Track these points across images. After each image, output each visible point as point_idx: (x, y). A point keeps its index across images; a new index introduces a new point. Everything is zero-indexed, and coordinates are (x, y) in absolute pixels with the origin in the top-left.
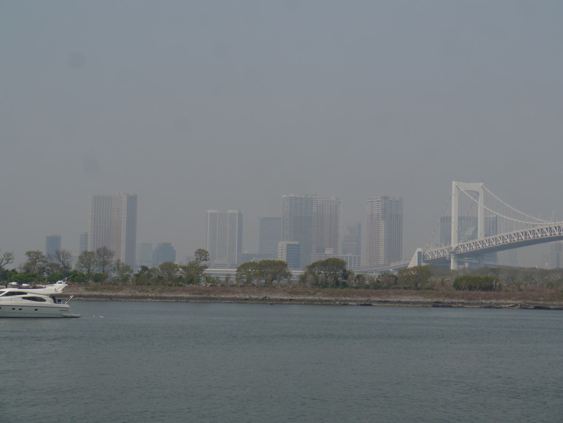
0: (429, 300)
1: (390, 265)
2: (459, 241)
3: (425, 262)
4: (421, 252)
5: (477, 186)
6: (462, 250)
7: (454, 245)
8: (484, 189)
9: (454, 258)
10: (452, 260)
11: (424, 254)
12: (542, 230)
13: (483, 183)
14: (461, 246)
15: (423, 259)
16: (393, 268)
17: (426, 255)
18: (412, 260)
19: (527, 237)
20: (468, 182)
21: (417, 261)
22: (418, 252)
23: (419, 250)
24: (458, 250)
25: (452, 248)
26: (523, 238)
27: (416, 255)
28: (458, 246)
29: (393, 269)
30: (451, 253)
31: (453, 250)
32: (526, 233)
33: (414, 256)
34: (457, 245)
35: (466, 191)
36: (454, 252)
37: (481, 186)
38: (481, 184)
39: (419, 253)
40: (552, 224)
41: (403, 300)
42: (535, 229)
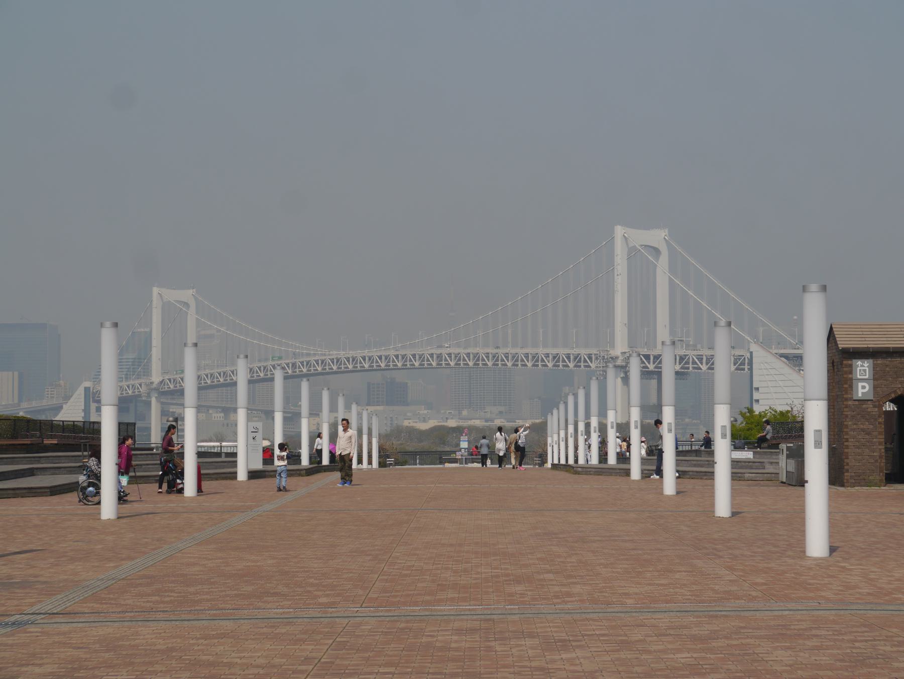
1: (19, 406)
2: (164, 373)
3: (95, 402)
4: (90, 388)
5: (187, 295)
6: (172, 386)
7: (156, 378)
8: (196, 299)
9: (156, 397)
10: (153, 400)
11: (94, 391)
12: (323, 362)
13: (194, 290)
14: (170, 380)
15: (93, 398)
16: (25, 410)
17: (97, 391)
18: (72, 400)
19: (297, 370)
20: (174, 289)
21: (83, 400)
22: (87, 389)
23: (88, 384)
24: (164, 384)
25: (152, 383)
27: (80, 391)
28: (161, 382)
29: (24, 412)
30: (152, 389)
31: (154, 386)
32: (294, 365)
33: (78, 392)
34: (161, 379)
35: (174, 301)
36: (155, 389)
37: (193, 295)
38: (191, 292)
39: (87, 389)
40: (342, 354)
42: (312, 359)
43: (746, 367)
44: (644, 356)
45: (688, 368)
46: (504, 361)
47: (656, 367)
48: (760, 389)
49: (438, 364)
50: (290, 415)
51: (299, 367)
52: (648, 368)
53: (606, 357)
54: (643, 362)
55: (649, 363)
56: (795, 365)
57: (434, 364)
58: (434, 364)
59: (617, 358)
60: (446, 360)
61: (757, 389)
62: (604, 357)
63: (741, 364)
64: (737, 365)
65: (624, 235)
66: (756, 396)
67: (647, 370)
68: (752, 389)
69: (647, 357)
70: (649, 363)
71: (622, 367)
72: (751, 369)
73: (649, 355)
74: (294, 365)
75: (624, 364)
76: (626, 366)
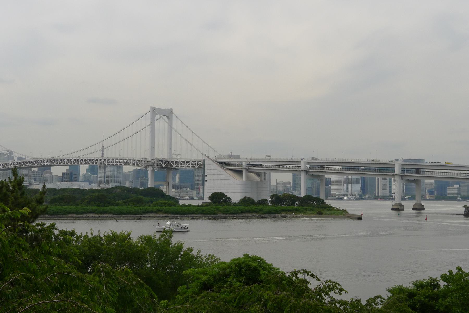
0: (161, 215)
26: (18, 166)
41: (150, 216)
43: (202, 166)
44: (161, 161)
45: (179, 166)
46: (104, 162)
47: (166, 166)
49: (78, 164)
50: (28, 185)
51: (22, 164)
52: (162, 166)
53: (145, 161)
54: (160, 164)
55: (163, 164)
56: (222, 166)
57: (76, 164)
58: (76, 164)
59: (150, 161)
60: (81, 162)
62: (144, 161)
63: (200, 165)
64: (198, 165)
65: (154, 111)
66: (206, 178)
67: (162, 167)
68: (204, 176)
69: (162, 161)
70: (163, 164)
71: (152, 166)
72: (204, 167)
73: (163, 161)
74: (20, 163)
75: (152, 164)
76: (153, 165)
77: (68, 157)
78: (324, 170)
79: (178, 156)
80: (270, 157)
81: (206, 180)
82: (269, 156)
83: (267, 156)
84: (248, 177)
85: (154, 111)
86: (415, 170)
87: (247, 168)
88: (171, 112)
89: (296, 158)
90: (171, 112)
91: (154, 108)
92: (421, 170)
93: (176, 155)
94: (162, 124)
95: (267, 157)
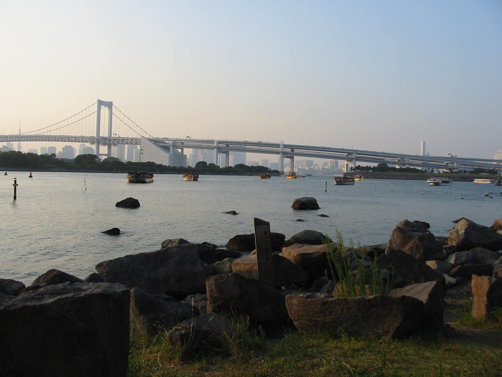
48: (144, 150)
61: (142, 150)
69: (106, 139)
77: (27, 134)
78: (228, 147)
79: (117, 136)
80: (189, 138)
81: (142, 153)
82: (189, 137)
83: (187, 137)
84: (173, 151)
85: (101, 103)
86: (290, 149)
87: (174, 145)
88: (111, 103)
89: (210, 138)
90: (111, 103)
91: (100, 100)
92: (295, 150)
93: (116, 135)
94: (105, 110)
95: (188, 138)
